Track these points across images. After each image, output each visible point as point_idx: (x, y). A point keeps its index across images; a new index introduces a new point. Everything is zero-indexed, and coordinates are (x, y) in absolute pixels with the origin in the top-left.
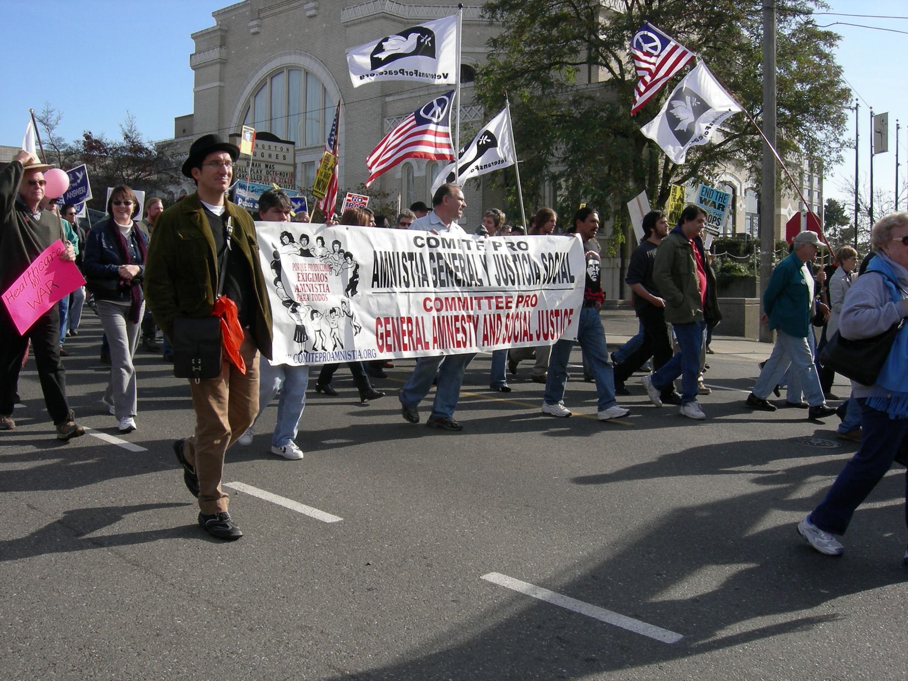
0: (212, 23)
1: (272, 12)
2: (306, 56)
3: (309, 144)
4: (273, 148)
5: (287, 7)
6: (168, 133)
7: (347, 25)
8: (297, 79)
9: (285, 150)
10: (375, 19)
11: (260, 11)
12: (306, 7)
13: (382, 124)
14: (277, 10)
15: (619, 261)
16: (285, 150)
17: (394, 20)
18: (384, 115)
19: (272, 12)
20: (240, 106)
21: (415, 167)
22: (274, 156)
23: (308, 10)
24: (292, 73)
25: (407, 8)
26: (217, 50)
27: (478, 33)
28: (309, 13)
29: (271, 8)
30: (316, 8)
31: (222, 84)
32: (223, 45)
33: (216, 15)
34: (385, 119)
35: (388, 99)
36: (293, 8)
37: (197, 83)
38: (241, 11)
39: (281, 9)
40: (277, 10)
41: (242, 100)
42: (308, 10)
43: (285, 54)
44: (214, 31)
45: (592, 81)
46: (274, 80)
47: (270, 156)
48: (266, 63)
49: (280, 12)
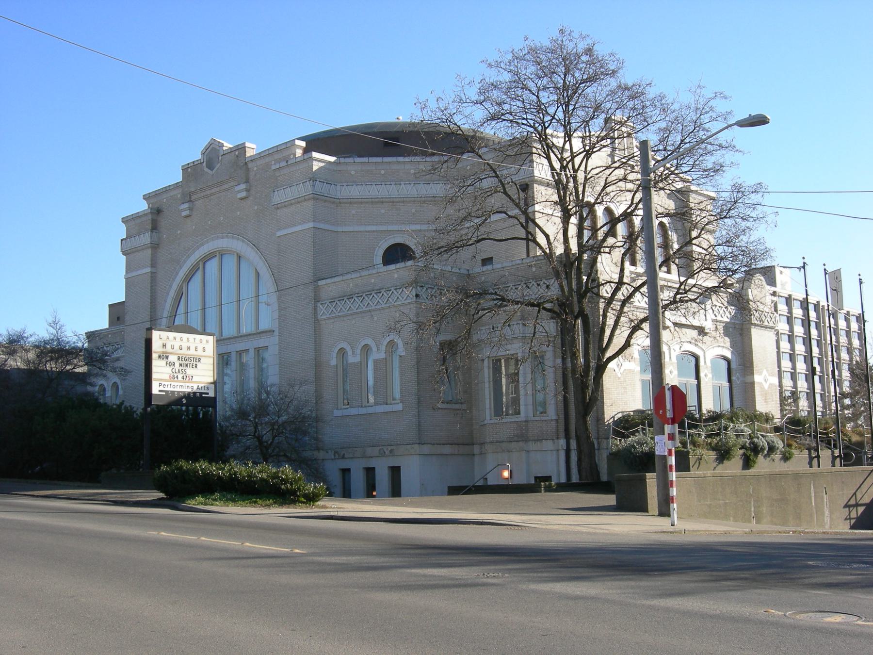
0: (143, 206)
1: (203, 194)
2: (238, 239)
3: (244, 331)
4: (192, 340)
5: (218, 189)
6: (102, 322)
7: (278, 207)
8: (230, 263)
9: (204, 342)
10: (305, 200)
11: (190, 194)
12: (237, 188)
13: (315, 309)
14: (208, 192)
15: (562, 442)
16: (204, 342)
17: (325, 201)
18: (317, 300)
19: (203, 194)
20: (172, 293)
21: (350, 353)
22: (200, 349)
23: (239, 192)
24: (225, 258)
25: (338, 187)
26: (148, 235)
27: (413, 211)
28: (239, 196)
29: (201, 190)
30: (248, 190)
31: (154, 270)
32: (155, 227)
33: (147, 197)
34: (319, 304)
35: (321, 283)
36: (225, 190)
37: (128, 269)
38: (172, 193)
39: (213, 191)
40: (208, 192)
41: (175, 287)
42: (239, 192)
43: (218, 238)
44: (145, 215)
45: (531, 255)
46: (208, 265)
47: (189, 348)
48: (198, 248)
49: (212, 195)
